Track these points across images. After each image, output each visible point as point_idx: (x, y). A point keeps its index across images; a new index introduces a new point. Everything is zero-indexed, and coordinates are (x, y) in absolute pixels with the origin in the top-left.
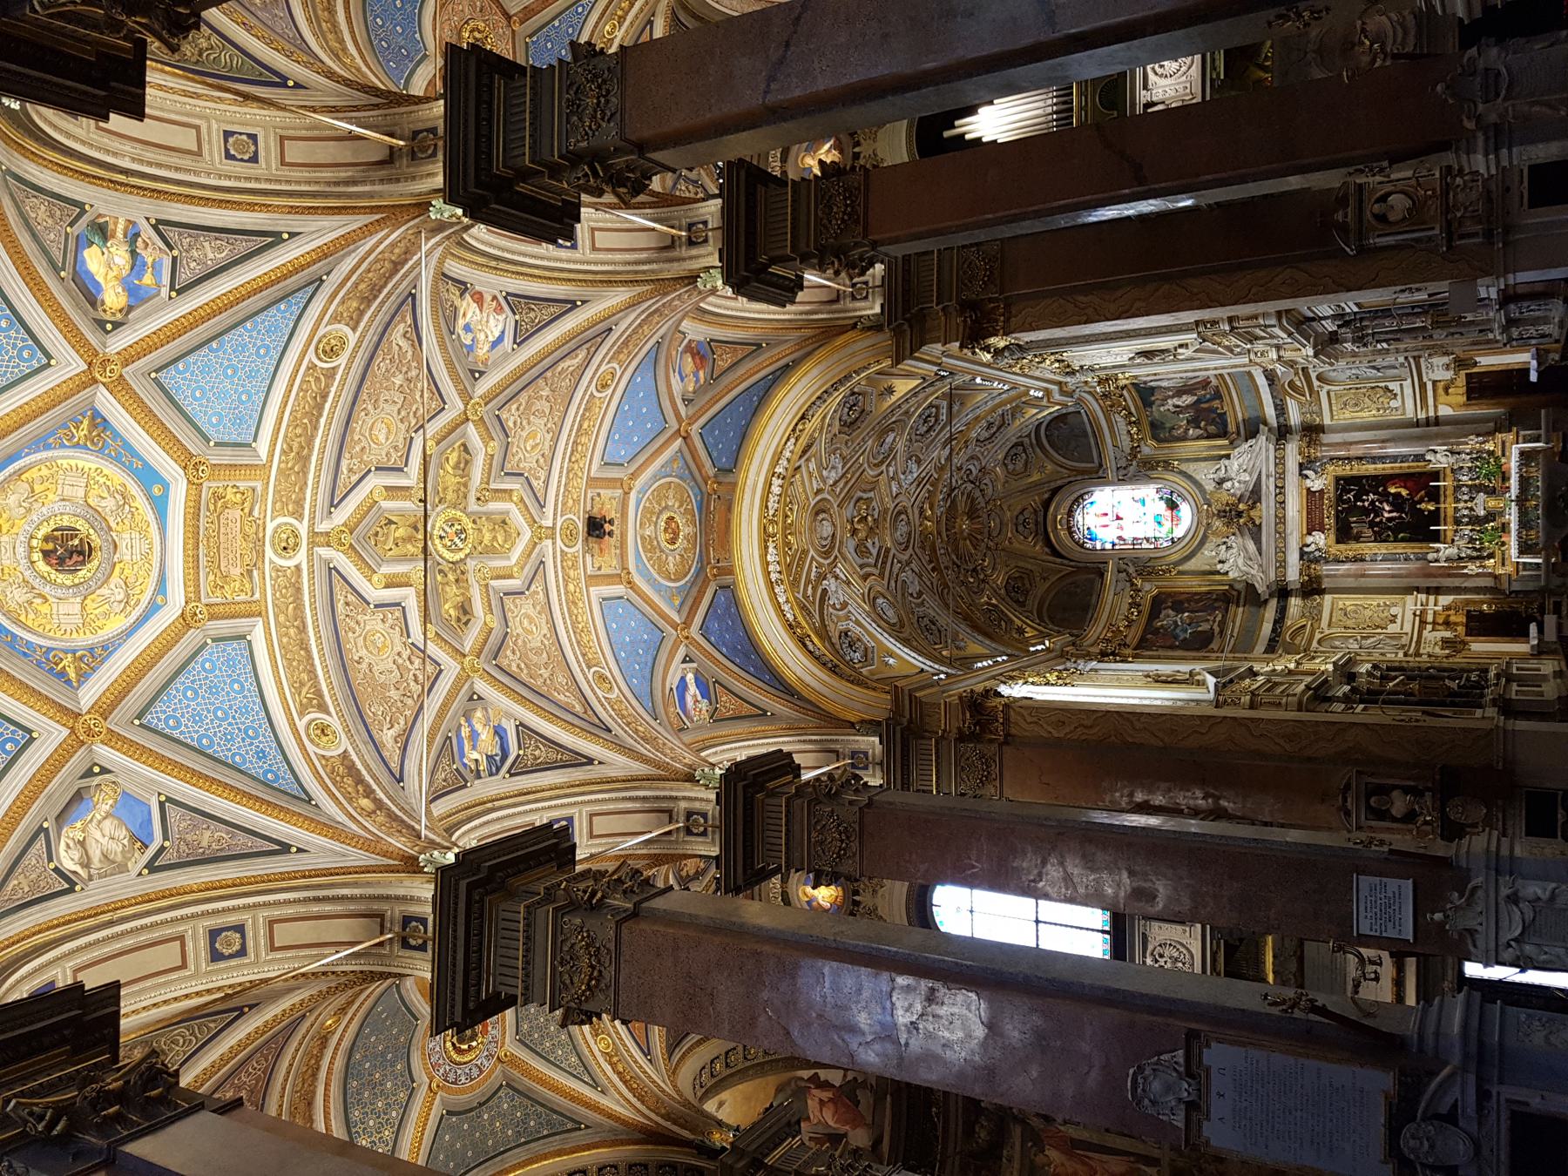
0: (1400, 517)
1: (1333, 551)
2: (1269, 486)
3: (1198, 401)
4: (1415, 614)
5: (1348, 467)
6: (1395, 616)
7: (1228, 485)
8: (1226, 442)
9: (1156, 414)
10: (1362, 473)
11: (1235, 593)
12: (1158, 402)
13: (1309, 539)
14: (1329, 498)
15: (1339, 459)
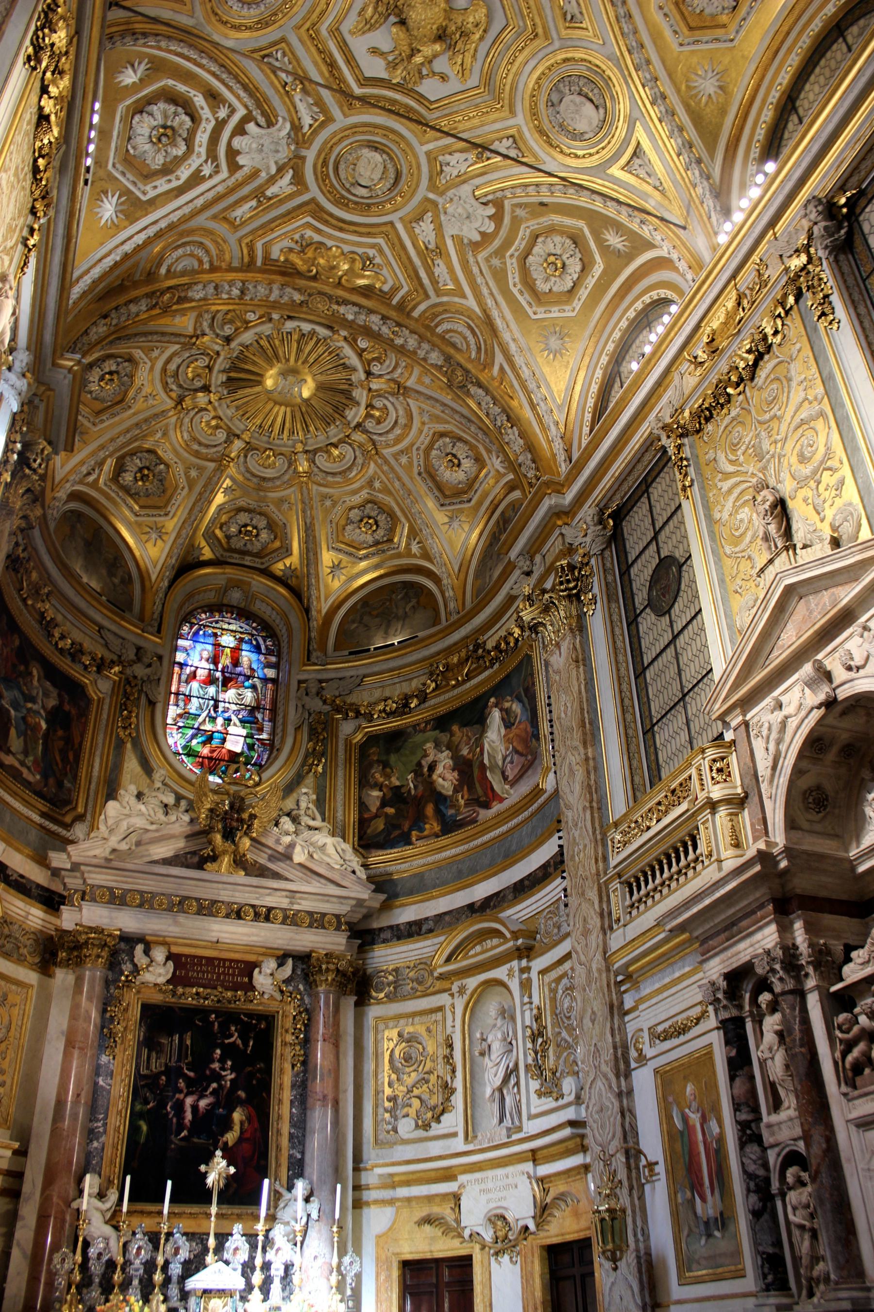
0: (181, 1127)
3: (439, 799)
5: (290, 1038)
7: (287, 824)
9: (419, 738)
11: (68, 819)
12: (444, 737)
13: (159, 954)
14: (236, 999)
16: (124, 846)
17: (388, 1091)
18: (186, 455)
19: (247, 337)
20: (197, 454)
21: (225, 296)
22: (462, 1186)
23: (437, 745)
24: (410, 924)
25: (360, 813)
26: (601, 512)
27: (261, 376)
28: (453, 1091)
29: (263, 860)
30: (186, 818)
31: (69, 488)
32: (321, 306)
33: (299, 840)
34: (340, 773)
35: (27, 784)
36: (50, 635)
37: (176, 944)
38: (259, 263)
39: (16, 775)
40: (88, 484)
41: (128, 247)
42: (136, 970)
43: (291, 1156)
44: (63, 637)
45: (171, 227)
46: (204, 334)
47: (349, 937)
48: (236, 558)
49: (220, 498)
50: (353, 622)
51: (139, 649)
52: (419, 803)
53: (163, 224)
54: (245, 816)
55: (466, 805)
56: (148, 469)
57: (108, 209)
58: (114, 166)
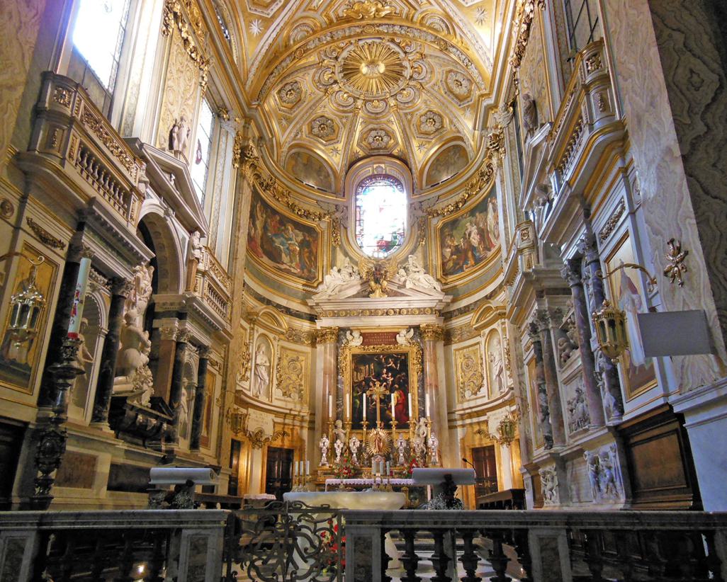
1: (347, 352)
2: (399, 303)
3: (473, 249)
4: (291, 410)
5: (415, 362)
6: (290, 397)
7: (402, 272)
8: (439, 277)
10: (410, 372)
11: (315, 285)
12: (474, 219)
13: (356, 334)
15: (422, 355)
16: (333, 293)
17: (461, 380)
18: (339, 113)
19: (345, 54)
20: (344, 112)
21: (325, 42)
22: (488, 417)
23: (471, 223)
24: (465, 307)
25: (442, 259)
26: (507, 104)
27: (358, 69)
28: (483, 379)
29: (395, 288)
30: (359, 277)
31: (287, 146)
32: (371, 30)
33: (408, 279)
34: (433, 243)
35: (294, 274)
36: (294, 210)
37: (363, 329)
38: (335, 21)
39: (288, 272)
40: (298, 139)
41: (270, 41)
42: (348, 341)
43: (419, 409)
44: (299, 210)
45: (286, 24)
46: (324, 60)
47: (440, 316)
48: (376, 152)
49: (359, 128)
50: (433, 170)
51: (336, 206)
52: (466, 251)
53: (282, 24)
54: (383, 272)
55: (483, 250)
56: (324, 124)
57: (255, 29)
58: (250, 9)
